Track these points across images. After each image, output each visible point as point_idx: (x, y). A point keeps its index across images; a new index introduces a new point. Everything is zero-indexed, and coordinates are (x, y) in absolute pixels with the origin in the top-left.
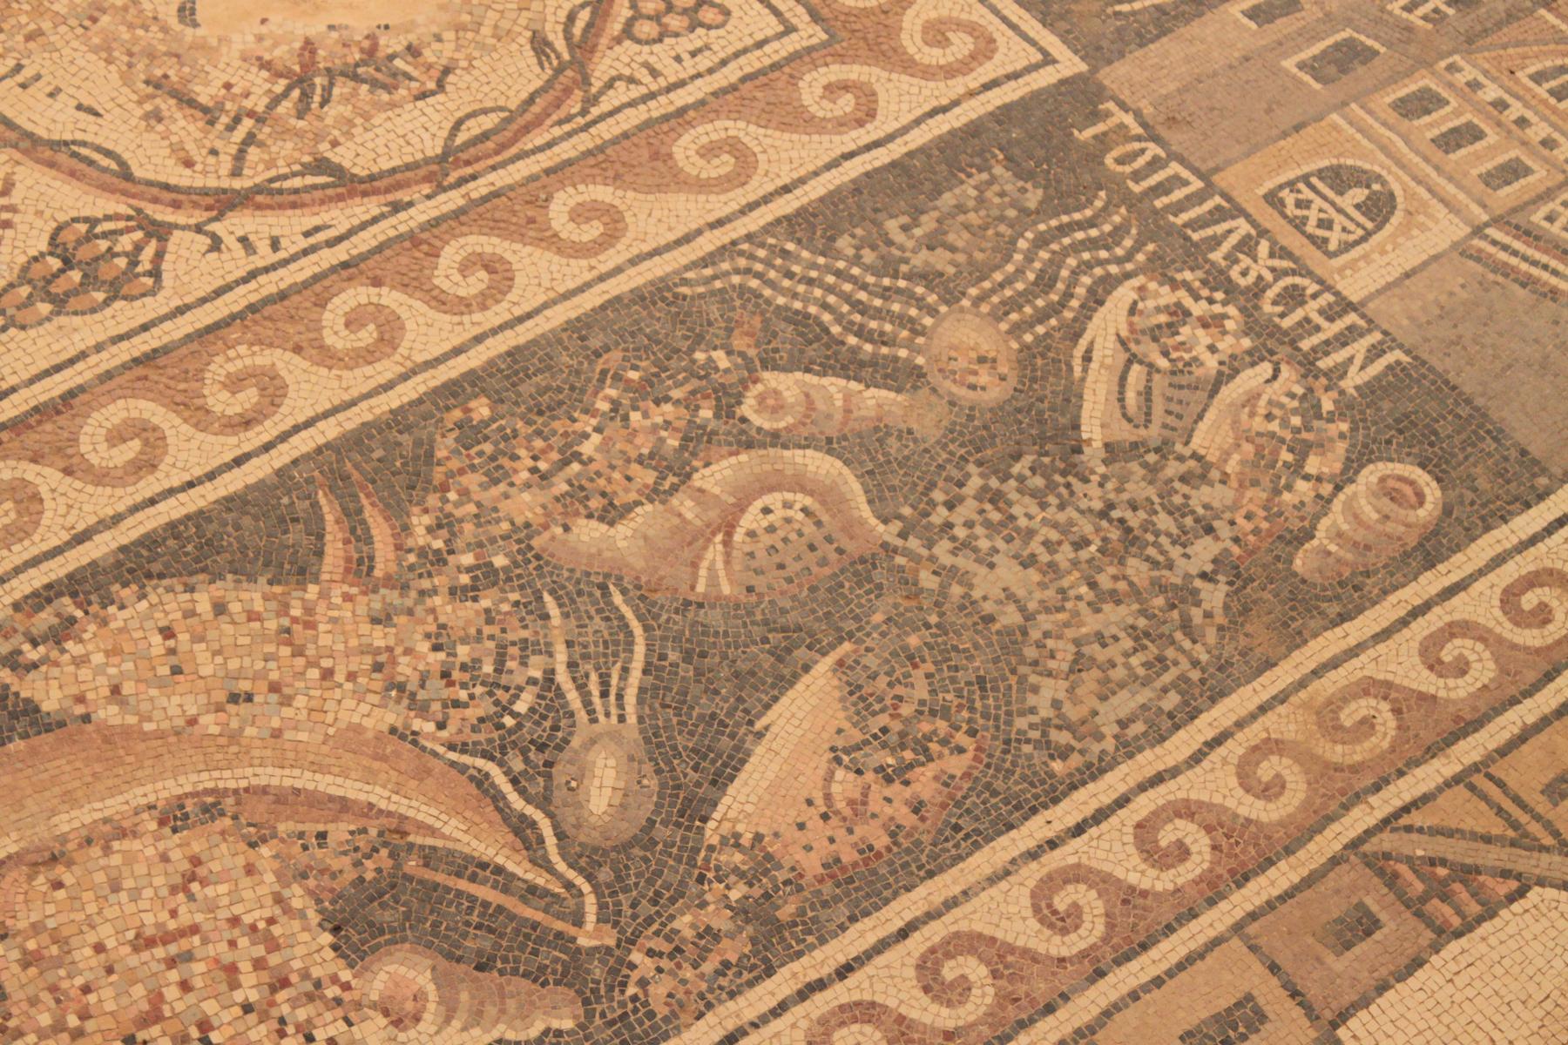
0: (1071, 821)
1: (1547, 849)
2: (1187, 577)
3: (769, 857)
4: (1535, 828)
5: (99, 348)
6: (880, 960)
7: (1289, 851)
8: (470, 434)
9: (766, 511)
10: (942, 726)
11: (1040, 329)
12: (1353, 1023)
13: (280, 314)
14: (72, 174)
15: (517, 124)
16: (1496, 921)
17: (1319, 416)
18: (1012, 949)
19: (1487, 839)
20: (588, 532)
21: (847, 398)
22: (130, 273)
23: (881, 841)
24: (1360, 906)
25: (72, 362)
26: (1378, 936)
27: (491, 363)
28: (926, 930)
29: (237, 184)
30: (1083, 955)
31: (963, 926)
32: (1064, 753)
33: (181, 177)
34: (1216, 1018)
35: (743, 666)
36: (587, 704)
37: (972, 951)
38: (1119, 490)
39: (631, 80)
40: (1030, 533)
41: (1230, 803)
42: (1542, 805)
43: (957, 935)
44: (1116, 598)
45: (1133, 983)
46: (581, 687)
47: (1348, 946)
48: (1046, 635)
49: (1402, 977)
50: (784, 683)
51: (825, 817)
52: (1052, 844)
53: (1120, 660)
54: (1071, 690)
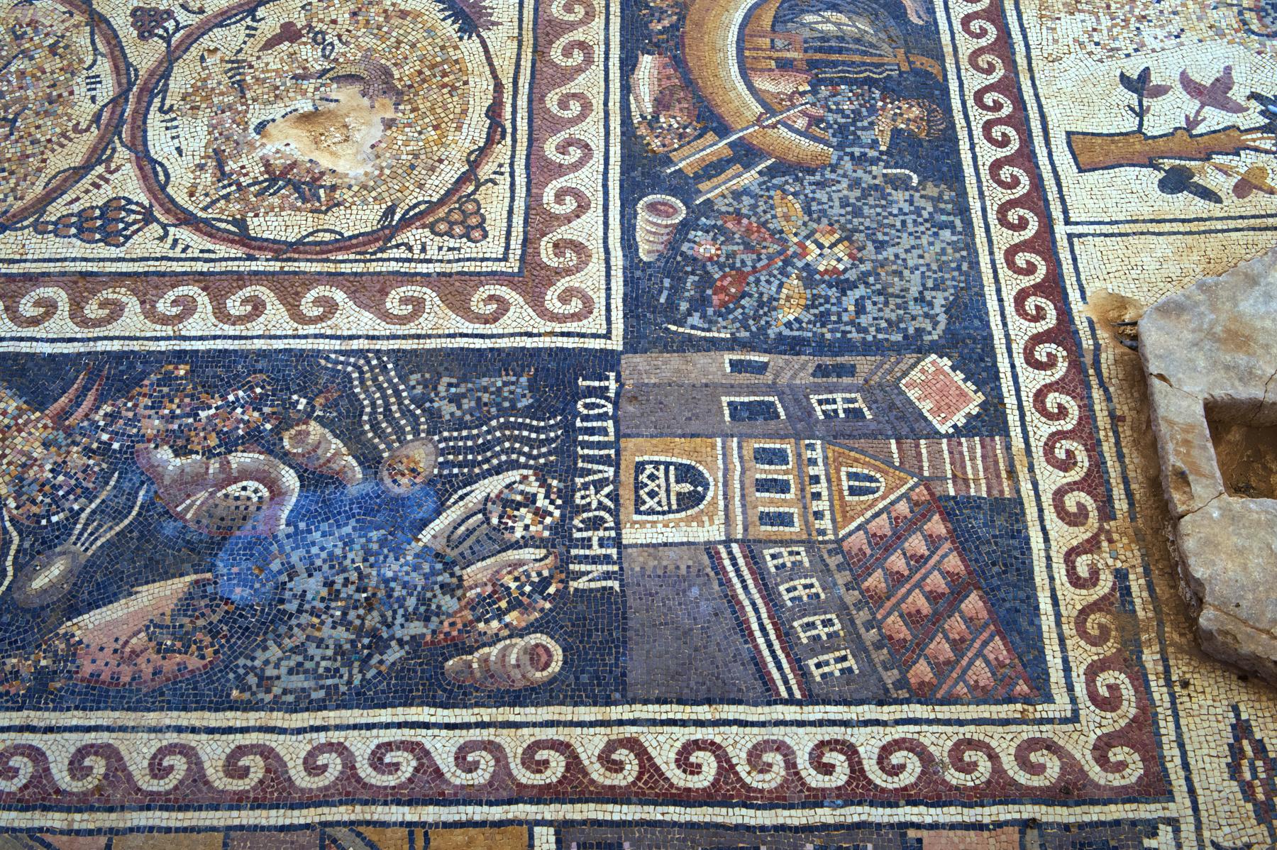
0: (213, 724)
2: (392, 638)
3: (74, 654)
5: (74, 260)
6: (67, 735)
7: (292, 807)
8: (168, 379)
9: (244, 489)
10: (208, 639)
11: (456, 471)
13: (148, 284)
14: (145, 178)
15: (343, 243)
17: (541, 593)
18: (124, 769)
20: (165, 453)
21: (337, 453)
22: (119, 233)
23: (126, 679)
25: (58, 260)
27: (209, 351)
28: (100, 734)
29: (200, 214)
30: (151, 793)
31: (116, 743)
33: (182, 199)
35: (158, 557)
36: (81, 534)
37: (108, 758)
38: (407, 573)
39: (410, 249)
40: (344, 570)
41: (290, 764)
43: (109, 746)
44: (348, 625)
45: (157, 823)
46: (86, 525)
48: (299, 625)
50: (166, 576)
51: (115, 651)
52: (194, 730)
53: (317, 659)
54: (280, 660)
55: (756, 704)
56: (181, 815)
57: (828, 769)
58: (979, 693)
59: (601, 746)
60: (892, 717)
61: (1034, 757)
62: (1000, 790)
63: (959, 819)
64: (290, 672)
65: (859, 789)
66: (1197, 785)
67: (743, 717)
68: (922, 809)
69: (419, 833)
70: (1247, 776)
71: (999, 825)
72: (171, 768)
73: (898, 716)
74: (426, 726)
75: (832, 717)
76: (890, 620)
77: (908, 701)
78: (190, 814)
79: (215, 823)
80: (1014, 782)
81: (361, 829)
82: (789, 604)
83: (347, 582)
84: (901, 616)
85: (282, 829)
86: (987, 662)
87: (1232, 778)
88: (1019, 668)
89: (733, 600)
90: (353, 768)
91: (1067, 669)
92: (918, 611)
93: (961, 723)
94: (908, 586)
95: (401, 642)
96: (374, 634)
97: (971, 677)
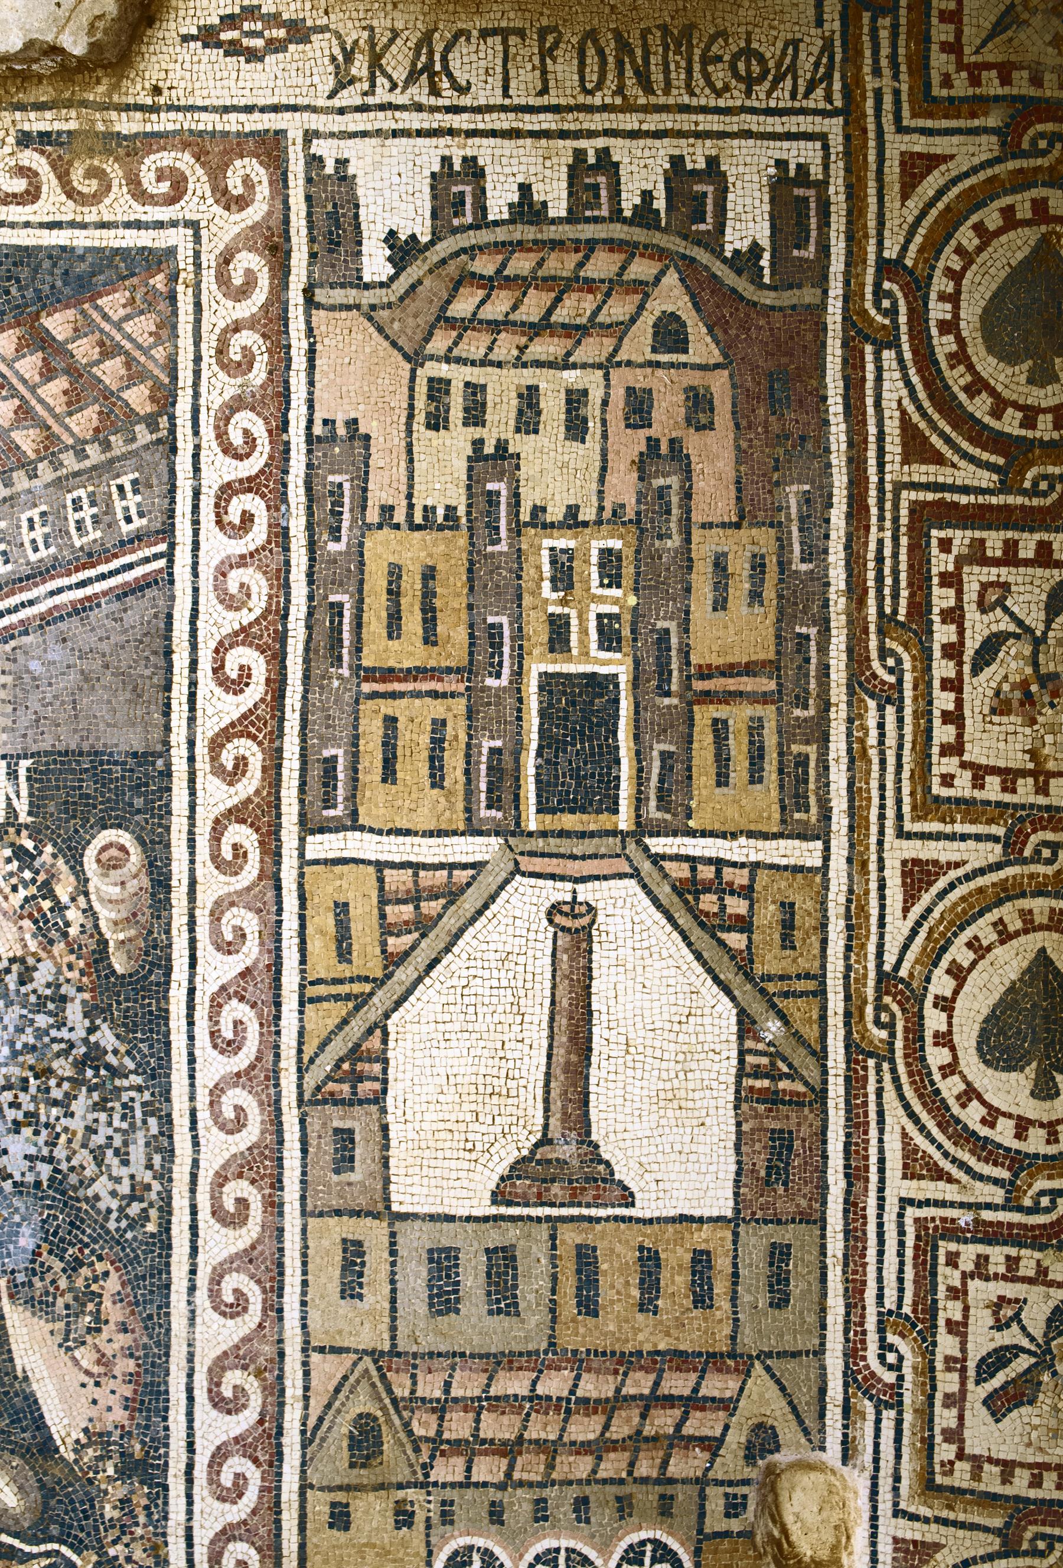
1: (371, 994)
2: (86, 1041)
4: (357, 988)
7: (281, 1142)
12: (394, 1197)
16: (392, 1063)
19: (345, 1022)
24: (337, 1131)
26: (357, 1137)
30: (264, 1310)
32: (144, 1216)
34: (344, 1268)
41: (234, 1150)
42: (345, 971)
44: (70, 1097)
45: (297, 1298)
47: (352, 1159)
49: (386, 1147)
53: (110, 1131)
55: (173, 598)
56: (288, 1271)
57: (247, 518)
58: (164, 333)
59: (217, 781)
60: (190, 438)
61: (238, 280)
62: (273, 322)
63: (303, 375)
64: (125, 1163)
65: (269, 484)
66: (269, 101)
67: (187, 614)
68: (292, 415)
69: (311, 991)
70: (259, 43)
71: (310, 331)
72: (236, 1291)
73: (189, 431)
74: (192, 991)
75: (188, 509)
76: (76, 429)
77: (172, 418)
78: (287, 1261)
79: (298, 1230)
80: (265, 307)
81: (306, 1059)
82: (53, 550)
83: (15, 1105)
84: (70, 414)
85: (304, 1151)
86: (128, 318)
87: (261, 59)
88: (135, 280)
89: (46, 620)
90: (238, 1075)
91: (137, 225)
92: (65, 393)
93: (198, 359)
94: (33, 402)
95: (92, 1030)
96: (80, 1065)
97: (147, 341)
